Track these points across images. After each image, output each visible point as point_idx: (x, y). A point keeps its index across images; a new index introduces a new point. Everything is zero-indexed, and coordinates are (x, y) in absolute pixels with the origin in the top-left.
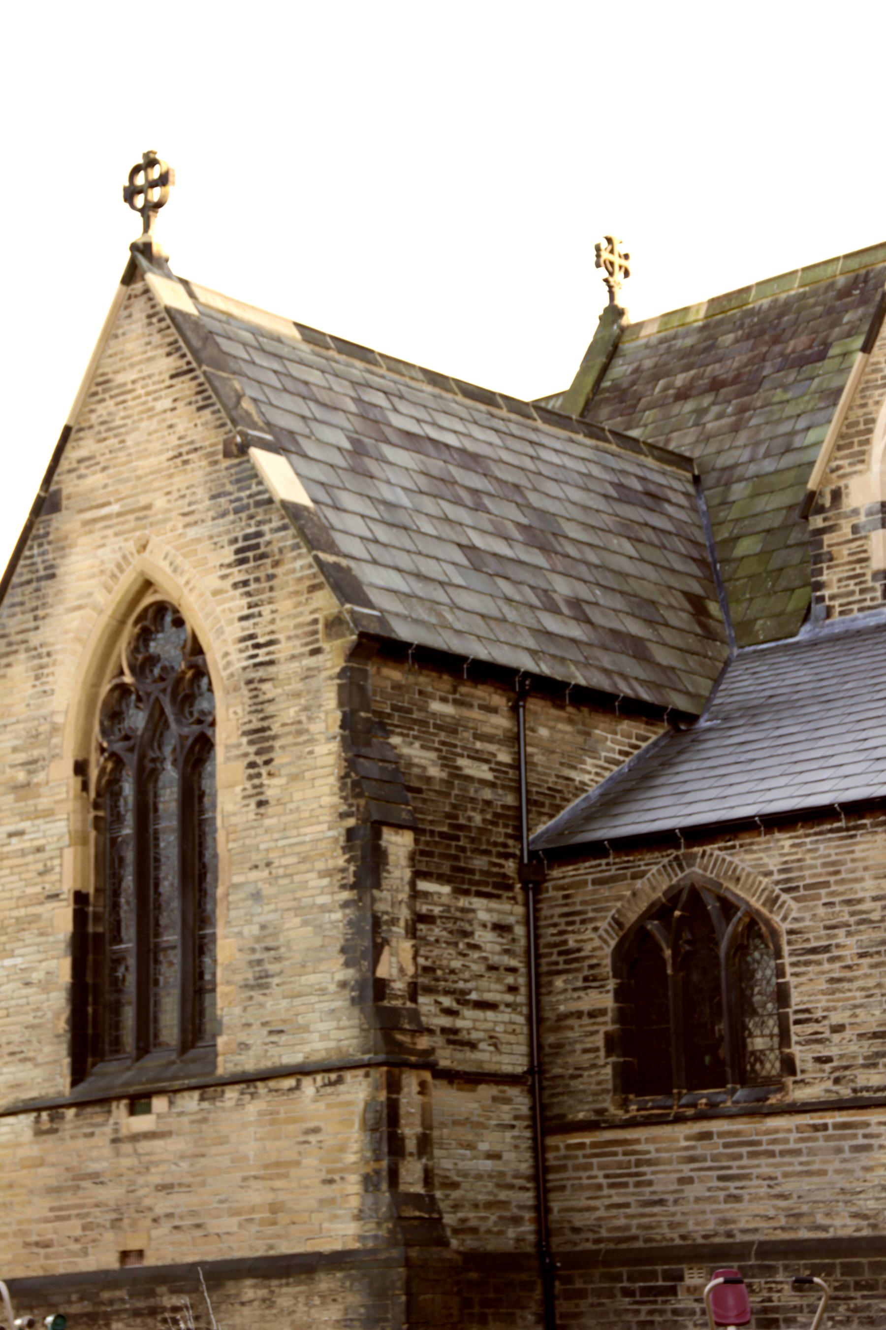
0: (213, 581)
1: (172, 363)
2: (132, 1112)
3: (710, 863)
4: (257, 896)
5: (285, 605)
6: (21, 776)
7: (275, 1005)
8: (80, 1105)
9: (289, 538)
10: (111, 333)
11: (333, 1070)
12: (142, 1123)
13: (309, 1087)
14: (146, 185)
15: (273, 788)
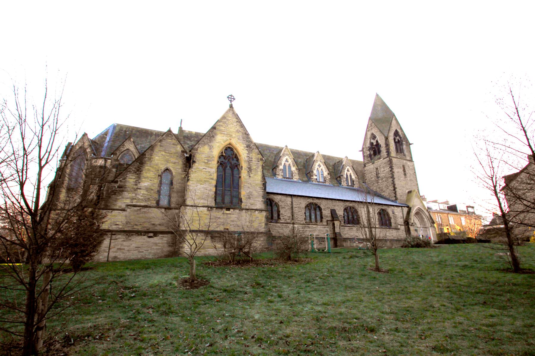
0: (243, 148)
1: (237, 120)
2: (227, 210)
3: (272, 196)
4: (249, 188)
5: (254, 155)
6: (206, 161)
7: (251, 201)
8: (217, 208)
9: (255, 147)
10: (227, 112)
11: (261, 210)
12: (228, 212)
13: (257, 212)
14: (231, 98)
15: (251, 175)
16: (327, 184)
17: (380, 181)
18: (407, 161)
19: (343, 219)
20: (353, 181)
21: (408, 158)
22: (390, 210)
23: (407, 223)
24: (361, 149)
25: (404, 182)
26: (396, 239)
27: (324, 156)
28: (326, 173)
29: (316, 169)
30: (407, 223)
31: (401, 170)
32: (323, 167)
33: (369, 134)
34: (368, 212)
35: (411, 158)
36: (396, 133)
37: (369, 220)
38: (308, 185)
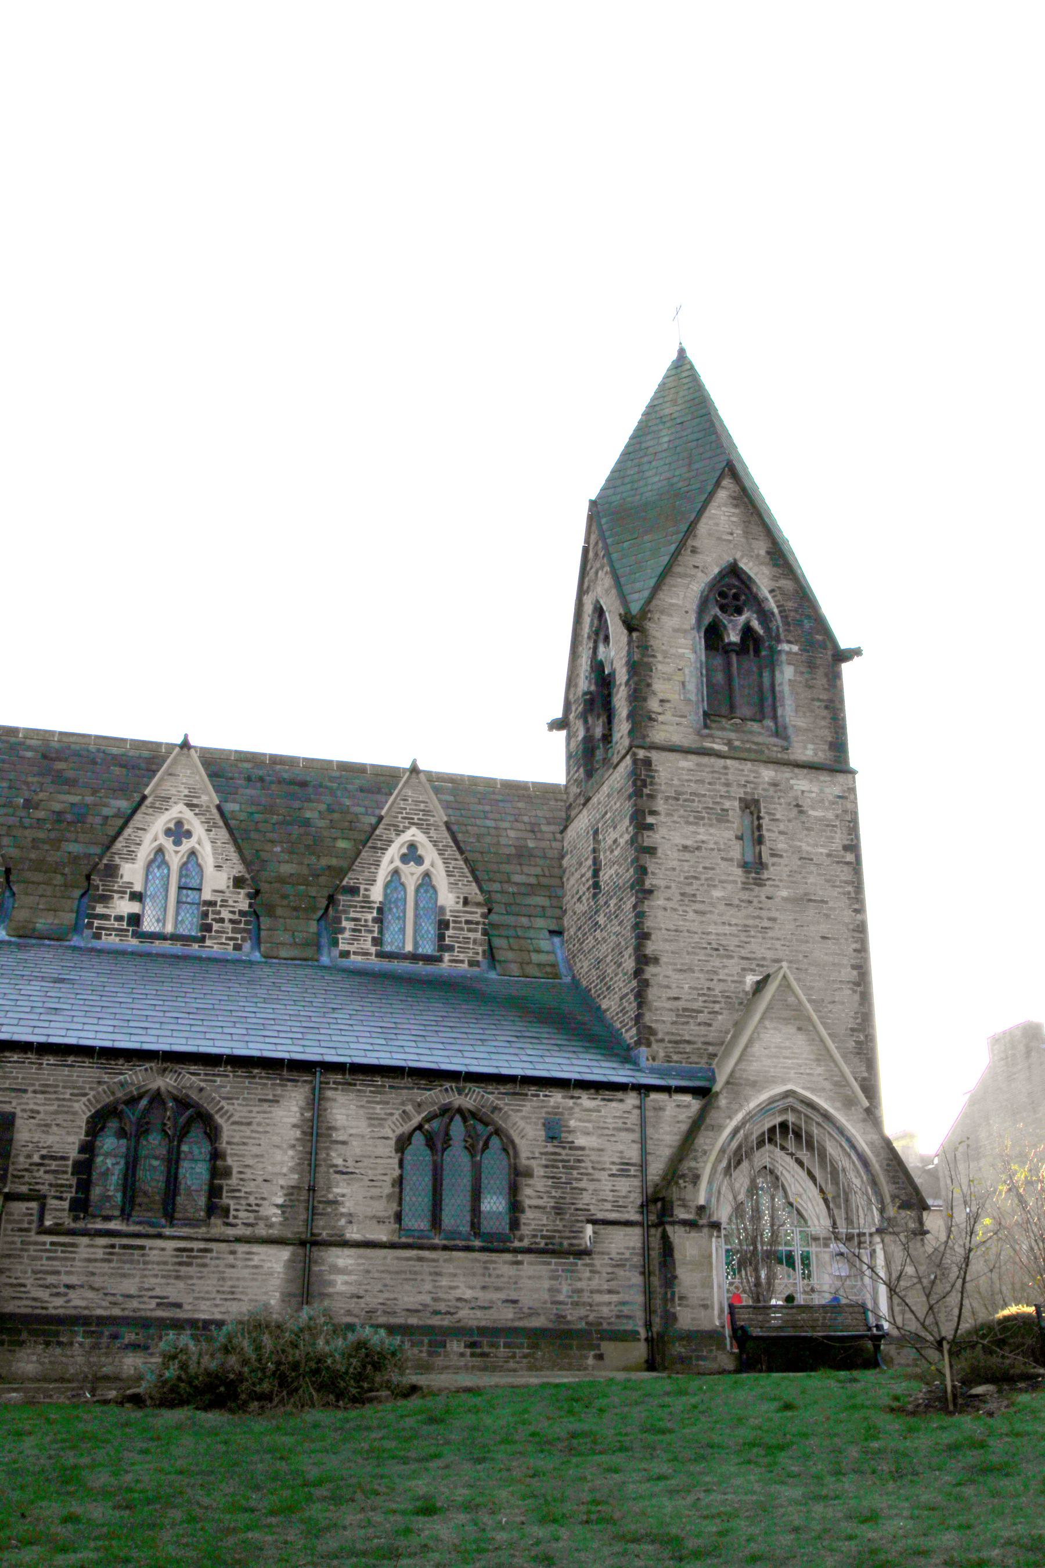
16: (213, 947)
17: (601, 920)
18: (786, 773)
19: (69, 1179)
20: (443, 925)
21: (806, 751)
22: (524, 1122)
23: (660, 1208)
24: (559, 714)
25: (738, 917)
26: (538, 1322)
27: (221, 768)
28: (217, 878)
29: (144, 852)
30: (660, 1208)
31: (724, 838)
32: (207, 843)
33: (588, 608)
34: (316, 1134)
35: (838, 746)
36: (731, 590)
37: (310, 1195)
38: (47, 960)
